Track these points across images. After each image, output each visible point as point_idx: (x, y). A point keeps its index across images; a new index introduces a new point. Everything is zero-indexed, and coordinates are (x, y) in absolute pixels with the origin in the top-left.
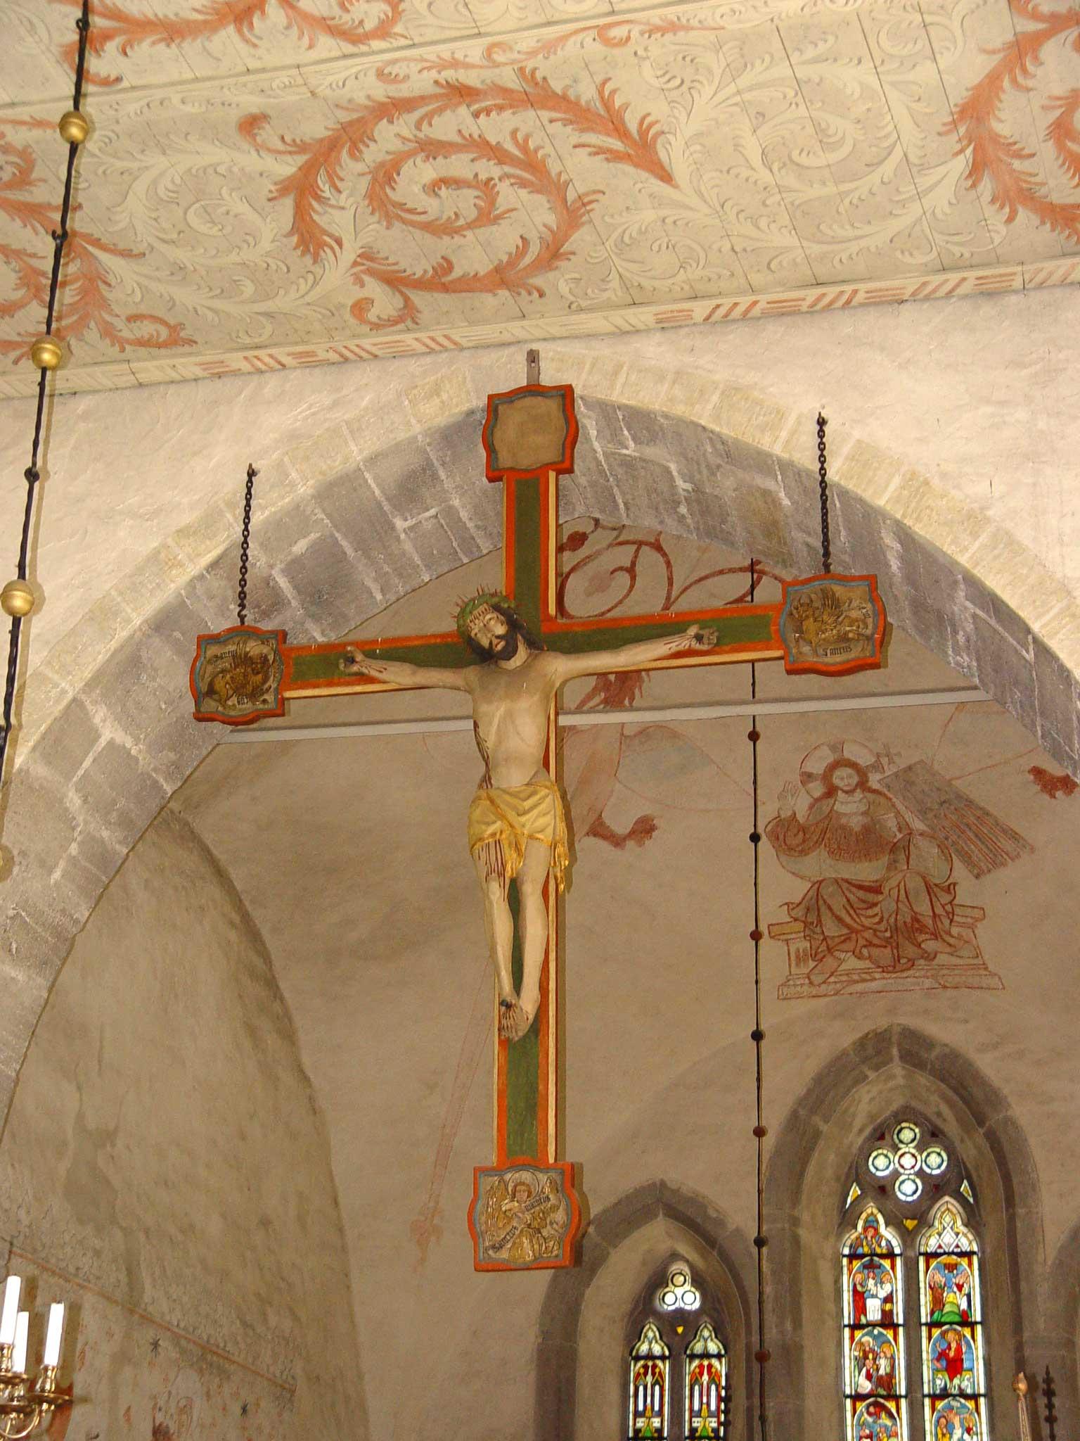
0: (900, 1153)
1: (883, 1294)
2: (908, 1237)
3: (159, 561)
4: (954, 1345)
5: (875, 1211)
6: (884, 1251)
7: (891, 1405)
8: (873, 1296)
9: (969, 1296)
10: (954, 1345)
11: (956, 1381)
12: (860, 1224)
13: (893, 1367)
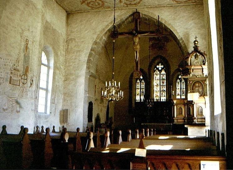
2: (160, 73)
3: (108, 25)
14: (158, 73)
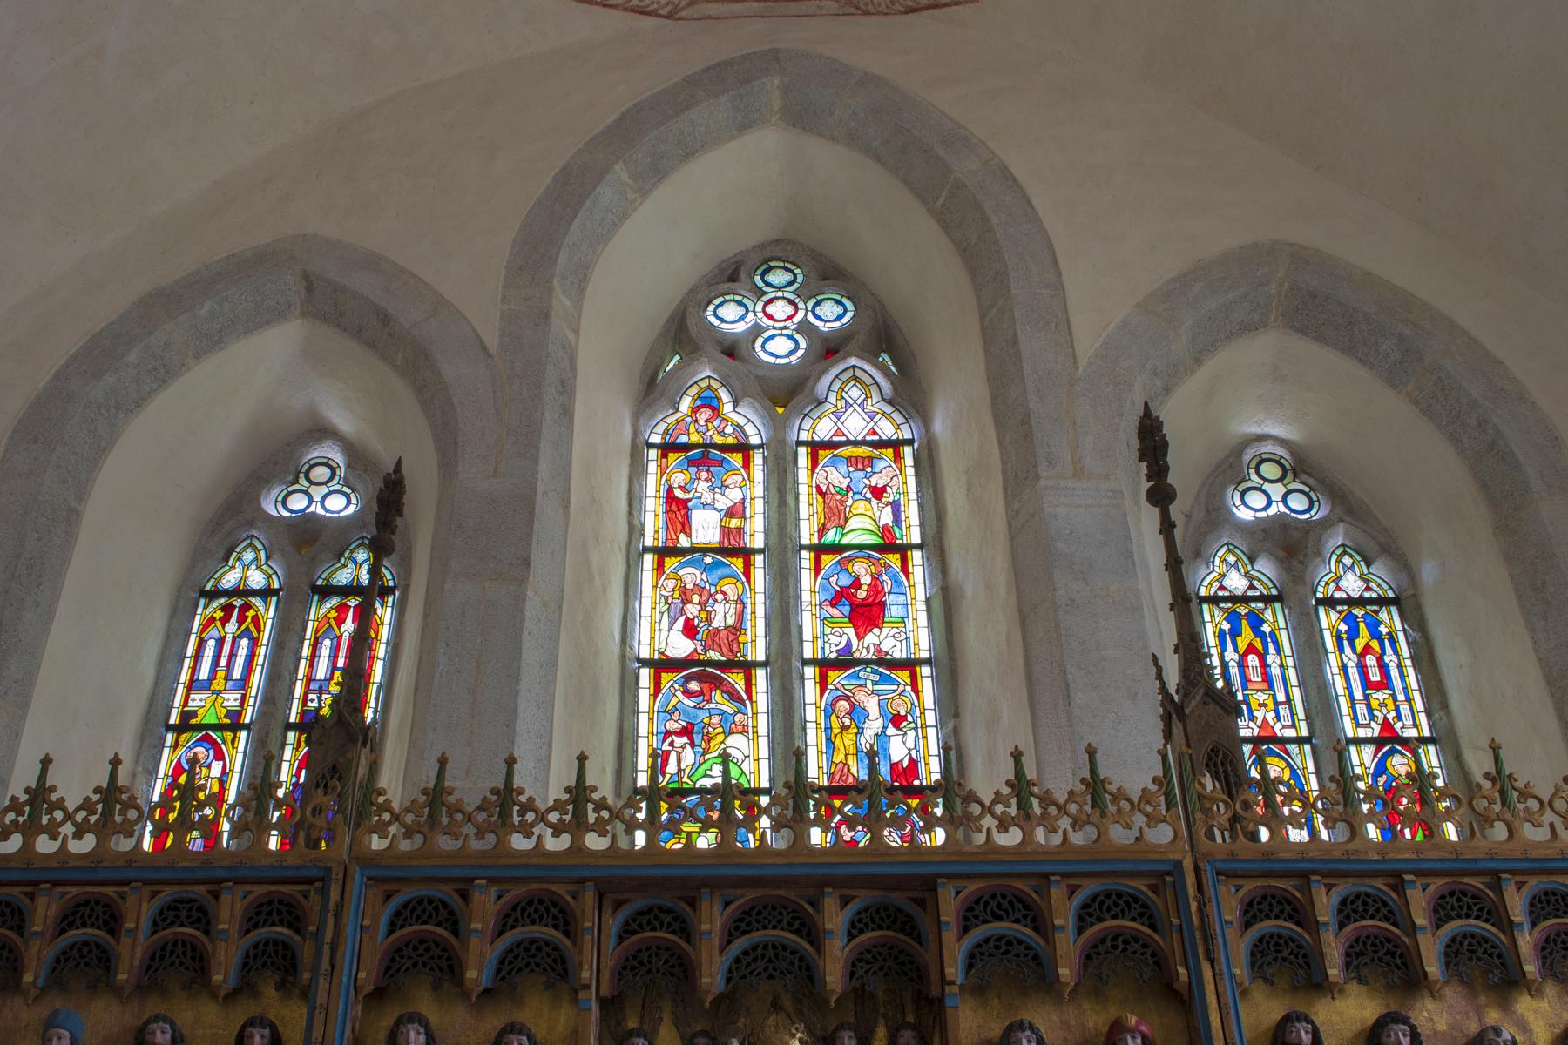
0: (765, 298)
1: (723, 503)
2: (778, 427)
4: (866, 580)
5: (715, 384)
6: (730, 441)
7: (737, 680)
8: (705, 506)
9: (896, 507)
10: (866, 580)
11: (870, 638)
12: (686, 405)
13: (740, 616)
14: (747, 421)
